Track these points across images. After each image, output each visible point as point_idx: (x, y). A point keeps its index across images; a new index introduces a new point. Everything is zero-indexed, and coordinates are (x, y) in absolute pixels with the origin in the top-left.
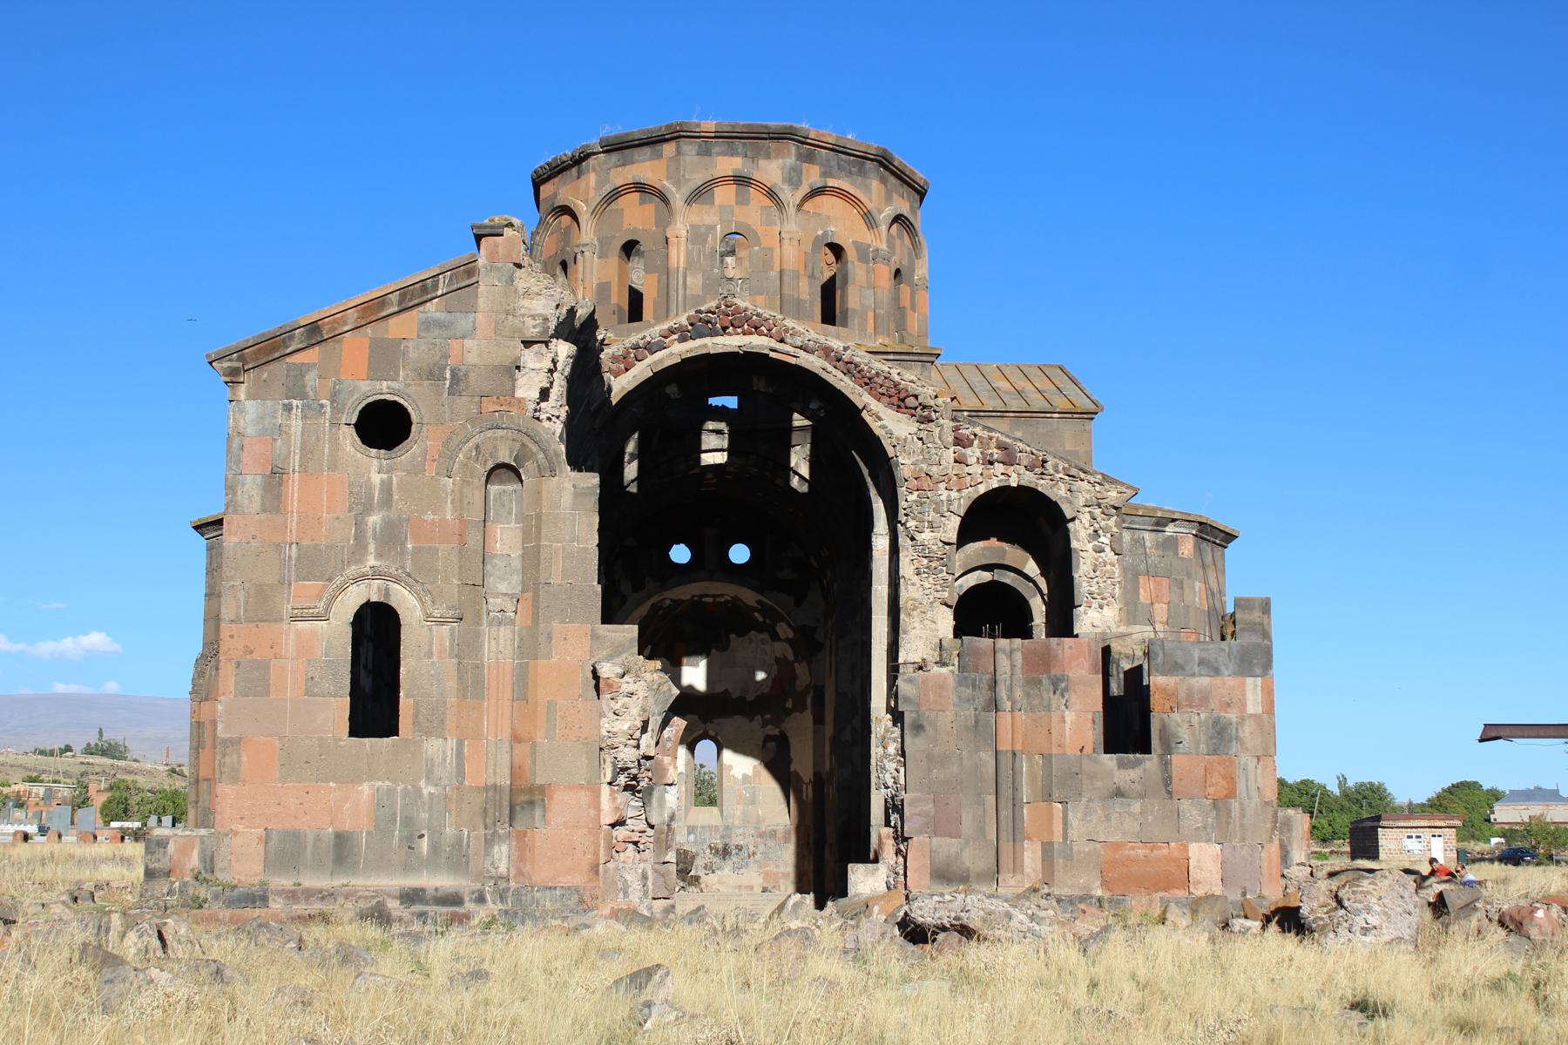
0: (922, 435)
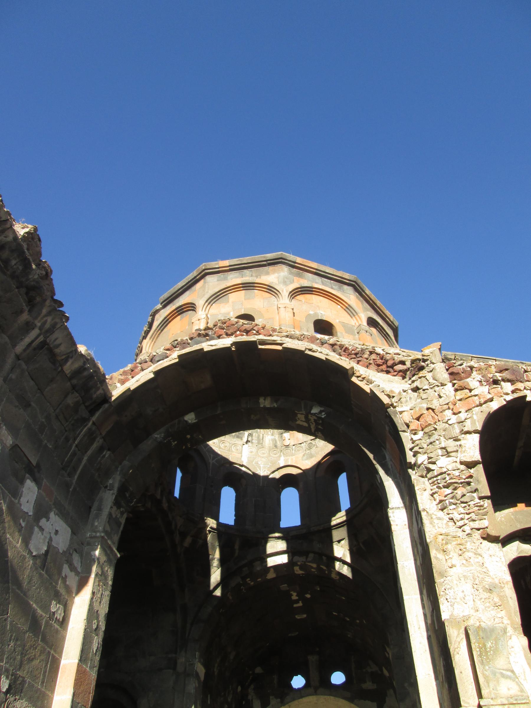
0: (414, 385)
